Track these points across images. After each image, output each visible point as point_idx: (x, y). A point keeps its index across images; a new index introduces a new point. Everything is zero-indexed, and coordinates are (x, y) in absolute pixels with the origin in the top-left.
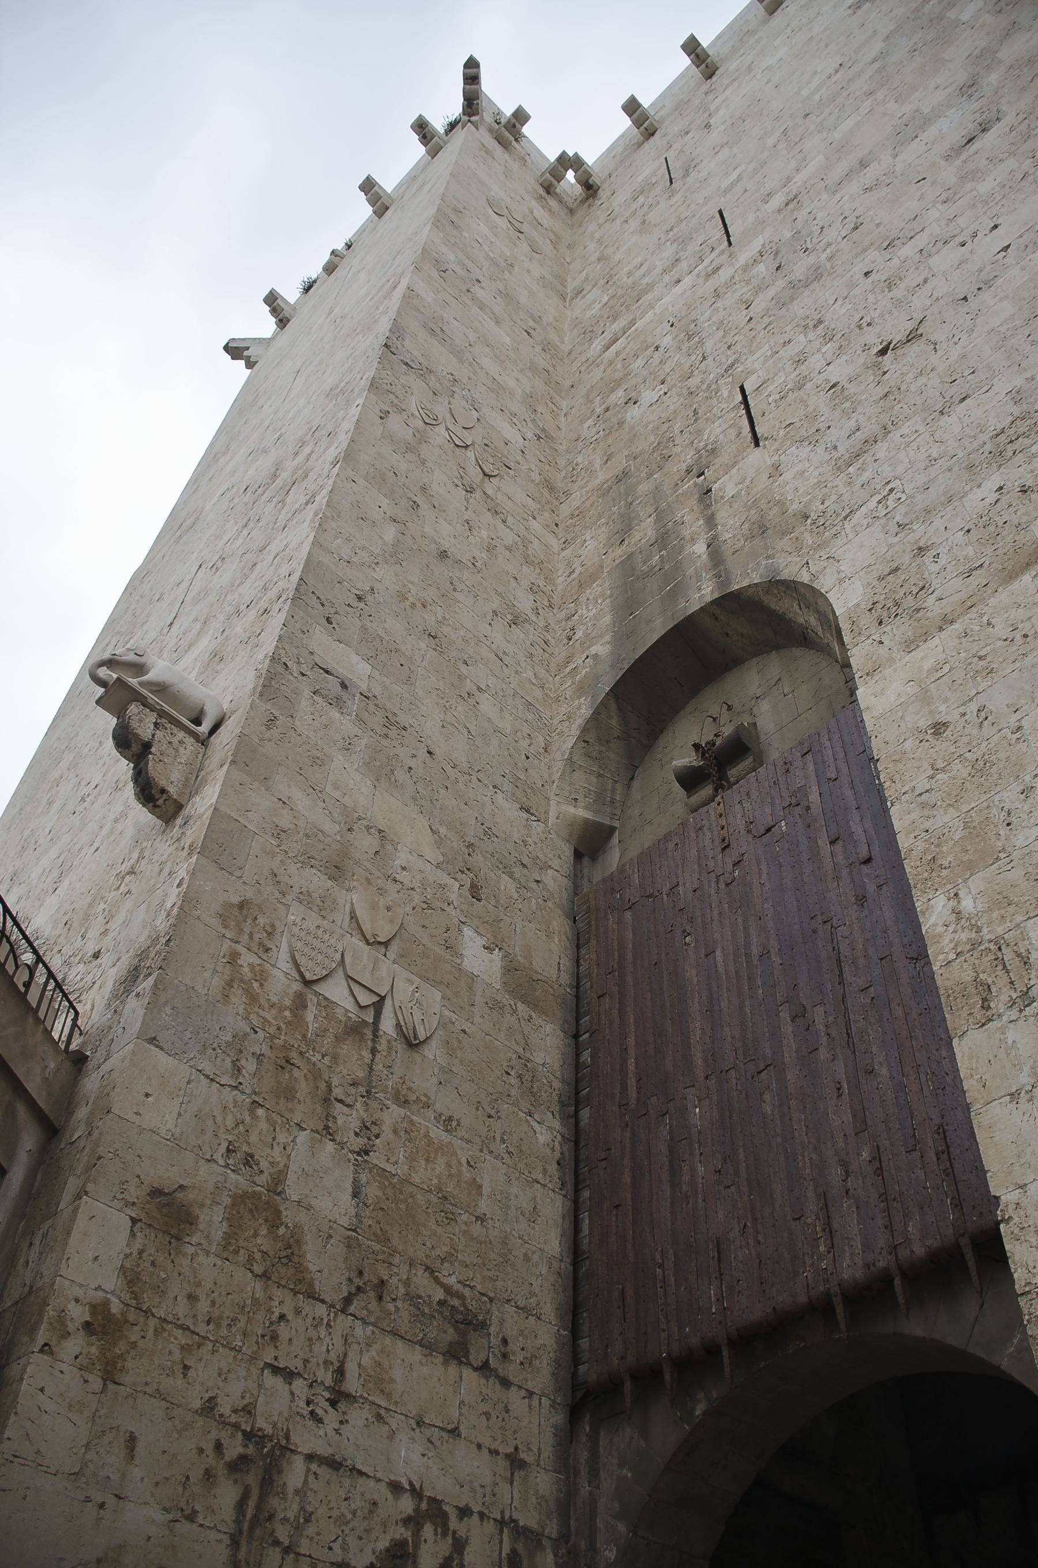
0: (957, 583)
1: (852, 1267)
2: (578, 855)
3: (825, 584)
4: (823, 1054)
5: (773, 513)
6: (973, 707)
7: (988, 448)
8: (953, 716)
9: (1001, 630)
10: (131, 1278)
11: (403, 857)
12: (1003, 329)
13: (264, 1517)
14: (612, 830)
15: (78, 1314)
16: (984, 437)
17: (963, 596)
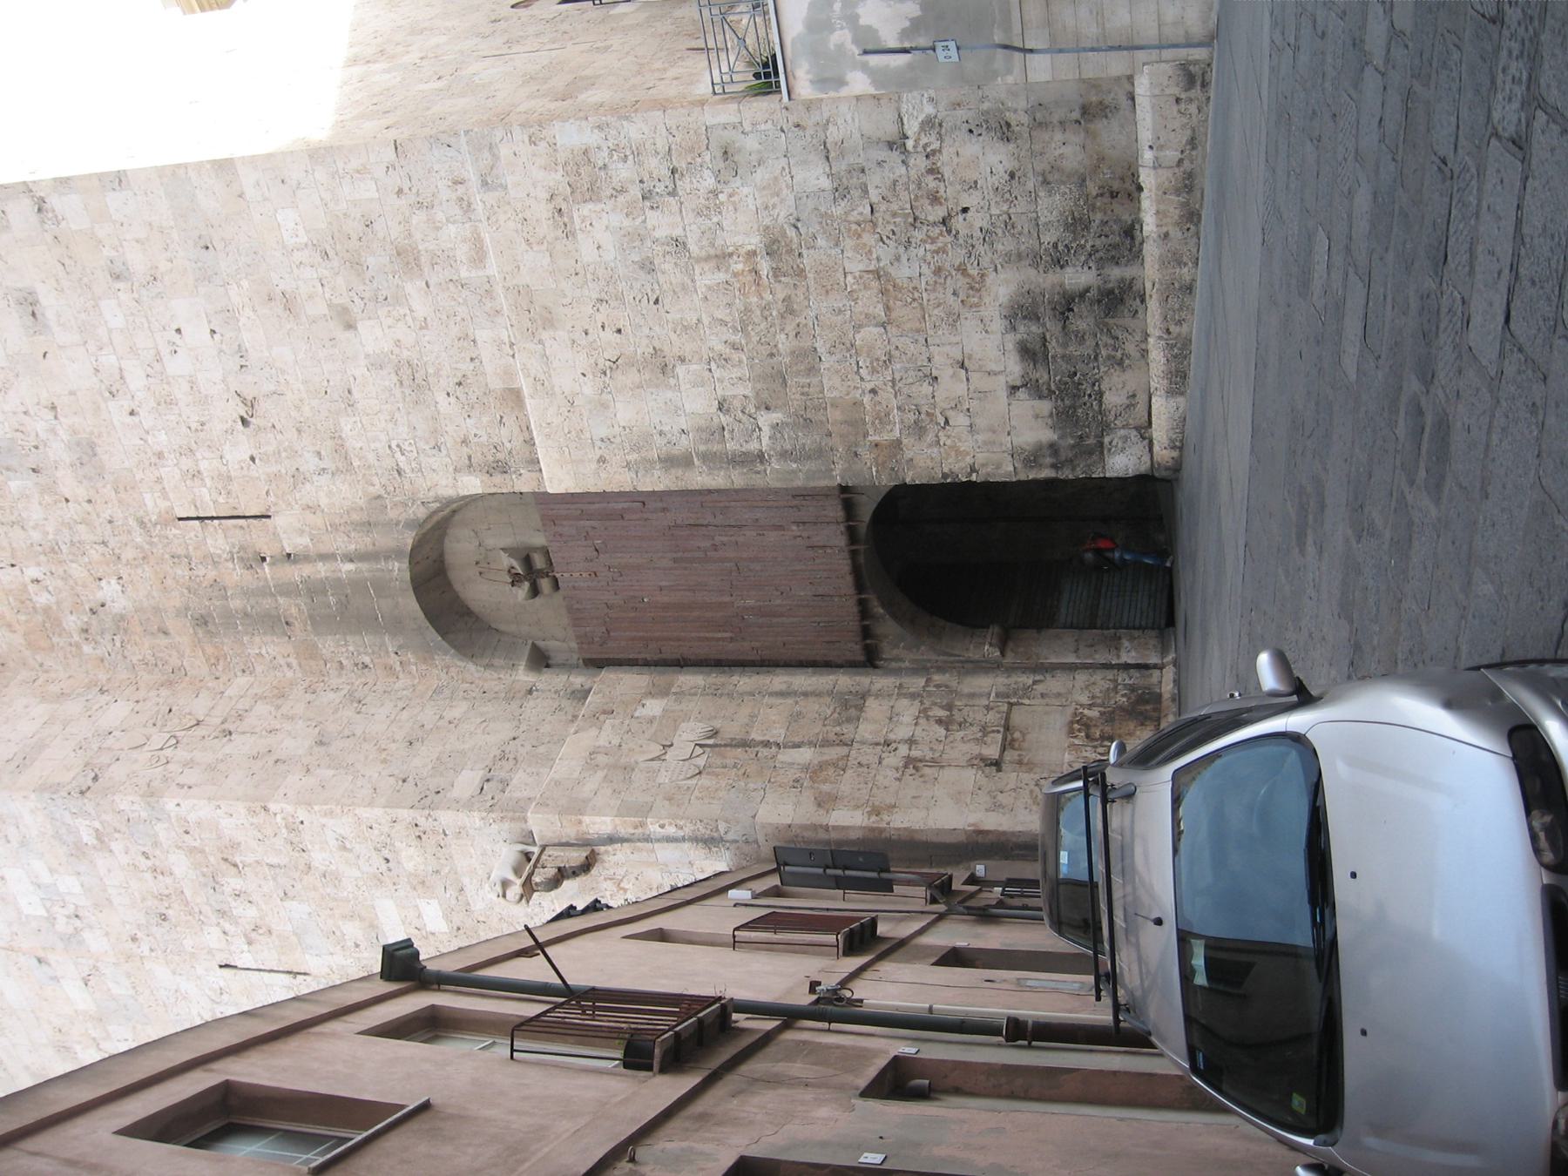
0: (504, 432)
1: (841, 541)
2: (548, 666)
4: (741, 539)
5: (355, 517)
6: (599, 443)
7: (408, 391)
8: (599, 453)
10: (857, 807)
11: (602, 742)
13: (933, 760)
14: (534, 645)
15: (874, 818)
16: (397, 392)
17: (516, 430)
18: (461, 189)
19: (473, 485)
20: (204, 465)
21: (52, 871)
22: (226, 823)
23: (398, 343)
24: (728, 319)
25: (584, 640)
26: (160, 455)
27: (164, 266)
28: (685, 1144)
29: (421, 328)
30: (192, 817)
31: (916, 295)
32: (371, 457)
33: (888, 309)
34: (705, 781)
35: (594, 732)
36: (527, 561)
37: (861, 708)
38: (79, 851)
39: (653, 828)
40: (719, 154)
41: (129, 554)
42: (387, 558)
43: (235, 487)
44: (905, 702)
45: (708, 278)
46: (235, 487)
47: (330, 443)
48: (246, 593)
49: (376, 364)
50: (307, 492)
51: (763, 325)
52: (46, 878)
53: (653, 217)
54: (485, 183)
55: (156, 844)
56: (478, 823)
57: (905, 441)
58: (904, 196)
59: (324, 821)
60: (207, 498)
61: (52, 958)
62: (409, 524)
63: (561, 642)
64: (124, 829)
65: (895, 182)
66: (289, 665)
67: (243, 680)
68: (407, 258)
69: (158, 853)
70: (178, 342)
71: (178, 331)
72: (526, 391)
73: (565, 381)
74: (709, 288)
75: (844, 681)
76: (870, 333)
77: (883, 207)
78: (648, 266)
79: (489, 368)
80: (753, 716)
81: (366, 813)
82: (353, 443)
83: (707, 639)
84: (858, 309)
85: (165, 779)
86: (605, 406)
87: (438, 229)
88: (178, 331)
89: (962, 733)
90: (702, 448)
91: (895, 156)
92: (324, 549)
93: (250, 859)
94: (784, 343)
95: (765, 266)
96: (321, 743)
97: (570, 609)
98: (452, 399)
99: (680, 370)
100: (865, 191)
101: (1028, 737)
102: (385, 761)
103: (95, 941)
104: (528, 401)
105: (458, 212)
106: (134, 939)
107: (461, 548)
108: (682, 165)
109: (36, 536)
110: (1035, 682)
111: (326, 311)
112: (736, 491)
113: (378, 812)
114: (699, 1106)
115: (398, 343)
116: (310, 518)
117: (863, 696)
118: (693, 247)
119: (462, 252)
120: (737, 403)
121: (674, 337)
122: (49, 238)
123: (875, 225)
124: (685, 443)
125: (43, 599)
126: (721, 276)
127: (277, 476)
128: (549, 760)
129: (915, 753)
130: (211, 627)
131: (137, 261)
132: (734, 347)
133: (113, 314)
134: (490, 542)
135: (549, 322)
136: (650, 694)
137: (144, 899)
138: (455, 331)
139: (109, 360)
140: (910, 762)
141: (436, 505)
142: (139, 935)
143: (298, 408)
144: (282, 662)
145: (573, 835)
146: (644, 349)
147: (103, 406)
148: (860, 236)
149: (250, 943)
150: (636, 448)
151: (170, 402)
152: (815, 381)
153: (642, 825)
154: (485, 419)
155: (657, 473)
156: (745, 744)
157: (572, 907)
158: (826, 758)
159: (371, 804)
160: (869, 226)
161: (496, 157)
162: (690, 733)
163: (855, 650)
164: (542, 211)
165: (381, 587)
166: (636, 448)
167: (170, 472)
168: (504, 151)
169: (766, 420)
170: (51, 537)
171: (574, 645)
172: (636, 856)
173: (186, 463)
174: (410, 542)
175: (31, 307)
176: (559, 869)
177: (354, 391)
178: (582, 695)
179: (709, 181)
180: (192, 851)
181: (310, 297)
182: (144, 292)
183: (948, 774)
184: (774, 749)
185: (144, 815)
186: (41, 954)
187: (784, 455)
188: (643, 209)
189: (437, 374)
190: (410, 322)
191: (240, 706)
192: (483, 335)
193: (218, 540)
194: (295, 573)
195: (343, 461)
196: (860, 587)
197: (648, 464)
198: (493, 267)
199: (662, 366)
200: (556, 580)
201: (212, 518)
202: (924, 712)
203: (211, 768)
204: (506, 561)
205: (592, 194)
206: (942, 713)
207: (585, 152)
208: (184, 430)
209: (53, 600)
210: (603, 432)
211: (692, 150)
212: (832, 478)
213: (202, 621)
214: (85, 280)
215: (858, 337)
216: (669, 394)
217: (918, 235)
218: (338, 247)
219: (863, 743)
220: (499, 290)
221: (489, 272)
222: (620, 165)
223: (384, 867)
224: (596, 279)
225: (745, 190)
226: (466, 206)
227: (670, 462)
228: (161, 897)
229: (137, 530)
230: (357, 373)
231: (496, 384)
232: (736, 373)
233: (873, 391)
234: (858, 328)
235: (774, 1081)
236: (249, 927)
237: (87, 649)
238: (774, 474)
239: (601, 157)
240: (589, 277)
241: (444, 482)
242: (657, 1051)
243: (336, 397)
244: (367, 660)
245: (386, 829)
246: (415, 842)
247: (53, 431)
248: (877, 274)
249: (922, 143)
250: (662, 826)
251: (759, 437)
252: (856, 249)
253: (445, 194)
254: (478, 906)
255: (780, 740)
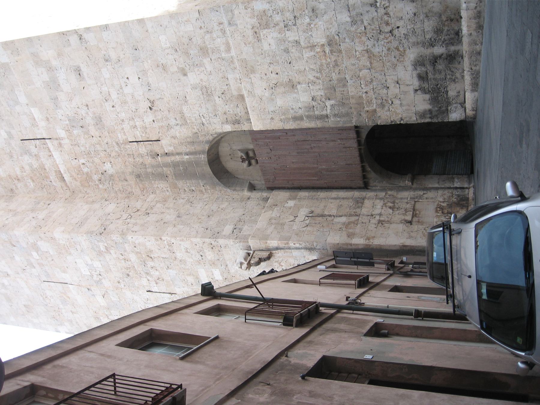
0: (238, 110)
1: (355, 145)
2: (255, 190)
3: (220, 131)
4: (320, 145)
5: (188, 140)
6: (271, 113)
7: (205, 96)
8: (271, 116)
9: (256, 105)
10: (362, 237)
11: (274, 215)
12: (169, 85)
13: (388, 221)
15: (367, 241)
16: (202, 97)
17: (242, 109)
18: (222, 26)
19: (228, 128)
20: (137, 124)
21: (92, 260)
22: (148, 244)
23: (201, 80)
24: (315, 68)
25: (267, 181)
26: (123, 121)
27: (122, 56)
28: (304, 351)
29: (209, 75)
30: (137, 242)
31: (381, 58)
32: (193, 119)
33: (371, 63)
34: (309, 228)
35: (271, 212)
36: (247, 154)
37: (363, 203)
38: (100, 253)
39: (291, 245)
40: (311, 10)
41: (113, 154)
42: (199, 154)
43: (148, 131)
44: (378, 201)
45: (307, 54)
46: (148, 131)
47: (179, 115)
48: (153, 166)
49: (194, 88)
50: (173, 132)
51: (327, 70)
52: (90, 262)
53: (288, 33)
54: (230, 24)
55: (125, 251)
56: (232, 243)
57: (378, 110)
58: (376, 23)
59: (180, 243)
60: (139, 135)
61: (92, 288)
62: (207, 142)
63: (259, 181)
64: (115, 246)
65: (373, 18)
66: (167, 191)
67: (152, 196)
68: (204, 51)
69: (126, 254)
70: (128, 82)
71: (128, 78)
72: (246, 96)
73: (259, 92)
74: (308, 58)
75: (357, 194)
76: (365, 72)
77: (369, 27)
78: (287, 51)
79: (233, 88)
80: (325, 206)
81: (194, 240)
82: (187, 115)
83: (309, 180)
84: (361, 63)
85: (128, 229)
86: (273, 100)
87: (214, 40)
88: (128, 78)
89: (398, 212)
90: (307, 114)
91: (373, 9)
92: (178, 151)
93: (156, 255)
94: (334, 76)
95: (327, 49)
96: (179, 217)
97: (262, 170)
98: (220, 99)
99: (299, 87)
100: (363, 22)
101: (421, 213)
102: (200, 222)
103: (106, 283)
104: (246, 99)
105: (221, 34)
106: (119, 282)
107: (224, 149)
108: (298, 15)
109: (83, 149)
110: (424, 194)
111: (177, 70)
112: (319, 128)
113: (198, 240)
114: (309, 338)
115: (201, 80)
116: (173, 141)
117: (364, 199)
118: (302, 43)
119: (223, 48)
120: (318, 98)
121: (296, 75)
122: (84, 48)
123: (366, 34)
124: (300, 112)
125: (86, 170)
126: (312, 53)
127: (162, 127)
128: (256, 222)
129: (382, 219)
130: (141, 178)
131: (113, 55)
132: (317, 78)
133: (106, 73)
134: (234, 148)
135: (253, 71)
136: (290, 199)
137: (122, 269)
138: (221, 75)
139: (105, 89)
140: (380, 222)
141: (216, 135)
142: (120, 281)
143: (168, 103)
144: (165, 189)
145: (264, 247)
146: (286, 79)
147: (103, 104)
148: (361, 38)
149: (157, 284)
150: (284, 114)
151: (125, 102)
152: (345, 89)
153: (287, 243)
154: (232, 106)
155: (291, 123)
156: (322, 216)
157: (264, 271)
158: (351, 220)
159: (196, 237)
160: (364, 34)
161: (233, 14)
162: (303, 212)
163: (361, 183)
164: (250, 33)
165: (198, 163)
166: (284, 114)
167: (126, 126)
168: (236, 12)
169: (329, 103)
170: (88, 149)
171: (263, 182)
172: (285, 254)
173: (132, 123)
174: (207, 148)
175: (78, 72)
176: (260, 258)
177: (187, 97)
178: (266, 199)
179: (308, 20)
180: (137, 253)
181: (172, 65)
182: (116, 65)
183: (393, 226)
184: (333, 217)
185: (121, 241)
186: (89, 287)
187: (335, 115)
188: (284, 31)
189: (215, 90)
190: (206, 73)
191: (152, 205)
192: (230, 76)
193: (143, 149)
194: (169, 159)
195: (184, 121)
196: (362, 161)
197: (288, 120)
198: (233, 53)
199: (292, 86)
200: (257, 160)
201: (141, 141)
202: (385, 204)
203: (142, 225)
204: (240, 154)
205: (267, 26)
206: (391, 205)
207: (264, 11)
208: (131, 112)
209: (89, 170)
210: (272, 109)
211: (301, 9)
212: (352, 123)
213: (138, 176)
214: (96, 62)
215: (360, 73)
216: (295, 95)
217: (382, 37)
218: (180, 48)
219: (363, 215)
220: (235, 60)
221: (232, 54)
222: (276, 15)
223: (201, 258)
224: (269, 56)
225: (320, 23)
226: (224, 32)
227: (296, 119)
228: (127, 268)
229: (116, 146)
230: (188, 91)
231: (235, 93)
232: (318, 87)
233: (366, 92)
234: (360, 70)
235: (334, 330)
236: (156, 278)
237: (101, 186)
238: (331, 122)
239: (270, 13)
240: (266, 55)
241: (218, 127)
242: (294, 320)
243: (181, 99)
244: (193, 188)
245: (201, 246)
246: (211, 250)
247: (87, 113)
248: (367, 51)
249: (382, 4)
250: (294, 244)
251: (326, 110)
252: (359, 42)
253: (216, 28)
254: (232, 271)
255: (335, 214)
